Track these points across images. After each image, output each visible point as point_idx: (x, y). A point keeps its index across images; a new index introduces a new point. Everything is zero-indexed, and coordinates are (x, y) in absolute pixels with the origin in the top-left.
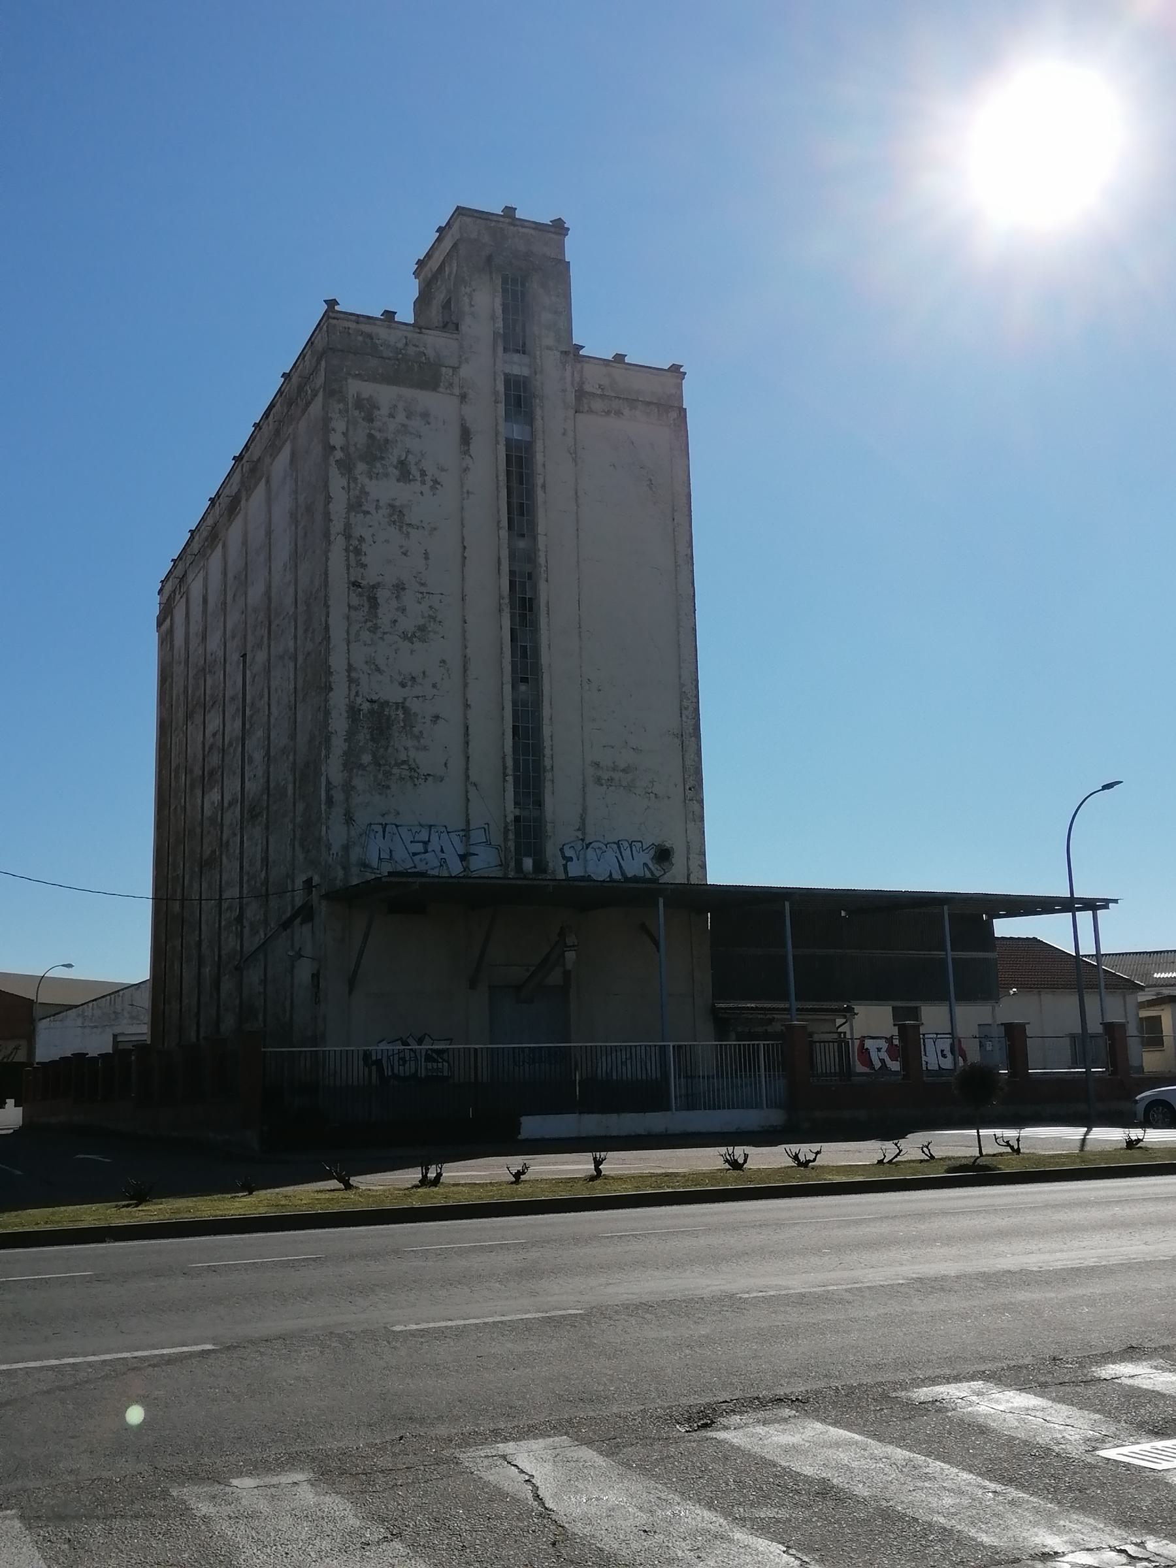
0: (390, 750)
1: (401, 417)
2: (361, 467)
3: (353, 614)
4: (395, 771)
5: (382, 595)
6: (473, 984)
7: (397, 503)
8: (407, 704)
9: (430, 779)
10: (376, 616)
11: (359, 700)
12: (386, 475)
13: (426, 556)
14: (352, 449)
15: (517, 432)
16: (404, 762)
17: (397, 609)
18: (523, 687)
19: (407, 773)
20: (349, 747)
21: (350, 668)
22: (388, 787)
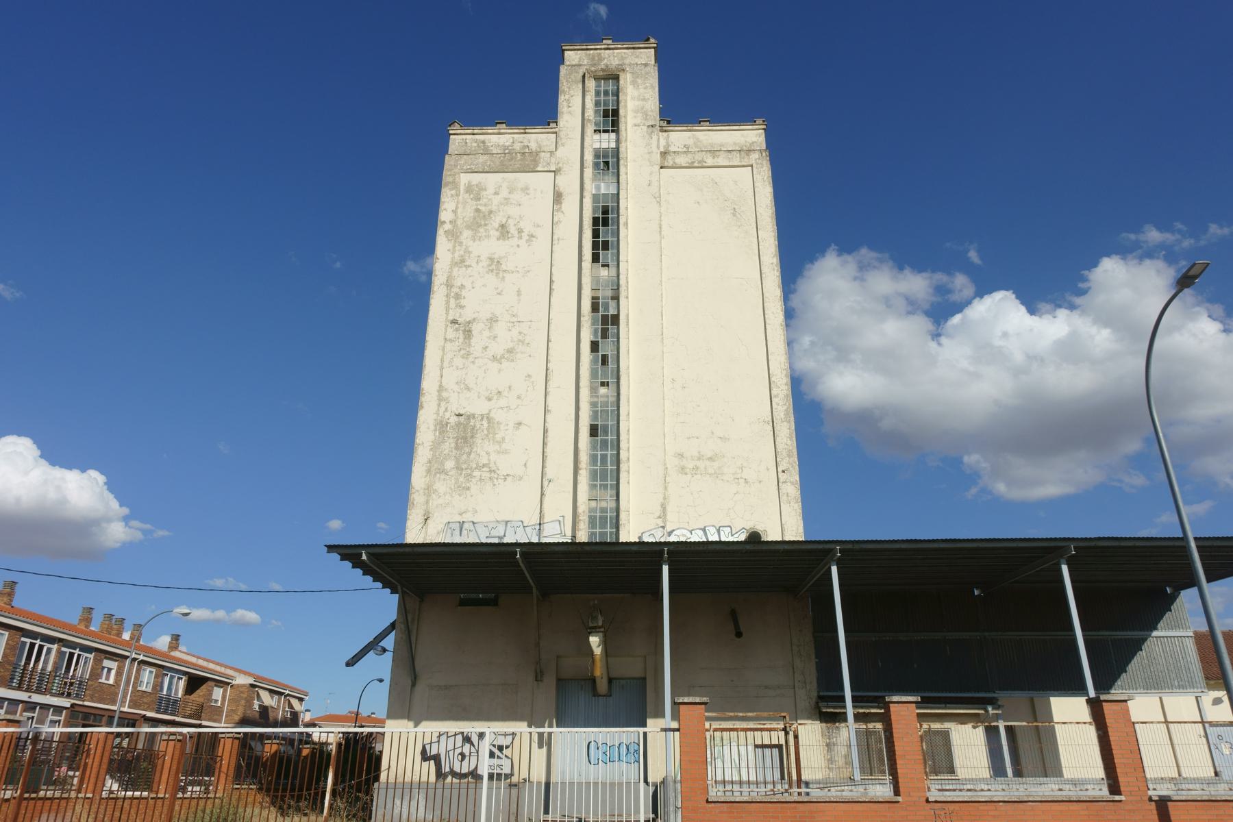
0: (473, 456)
1: (504, 193)
2: (467, 234)
3: (448, 345)
4: (476, 473)
5: (476, 328)
6: (539, 676)
7: (496, 256)
8: (492, 415)
9: (509, 479)
10: (470, 345)
11: (447, 415)
12: (488, 236)
13: (519, 293)
14: (459, 222)
15: (607, 188)
16: (484, 465)
17: (489, 338)
18: (603, 390)
19: (488, 475)
20: (434, 455)
21: (441, 388)
22: (468, 489)
